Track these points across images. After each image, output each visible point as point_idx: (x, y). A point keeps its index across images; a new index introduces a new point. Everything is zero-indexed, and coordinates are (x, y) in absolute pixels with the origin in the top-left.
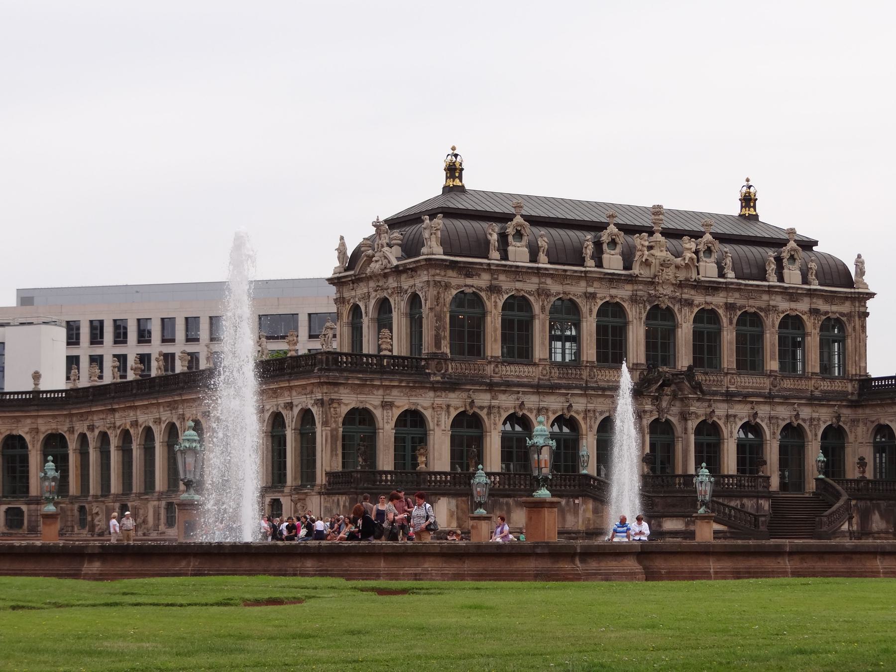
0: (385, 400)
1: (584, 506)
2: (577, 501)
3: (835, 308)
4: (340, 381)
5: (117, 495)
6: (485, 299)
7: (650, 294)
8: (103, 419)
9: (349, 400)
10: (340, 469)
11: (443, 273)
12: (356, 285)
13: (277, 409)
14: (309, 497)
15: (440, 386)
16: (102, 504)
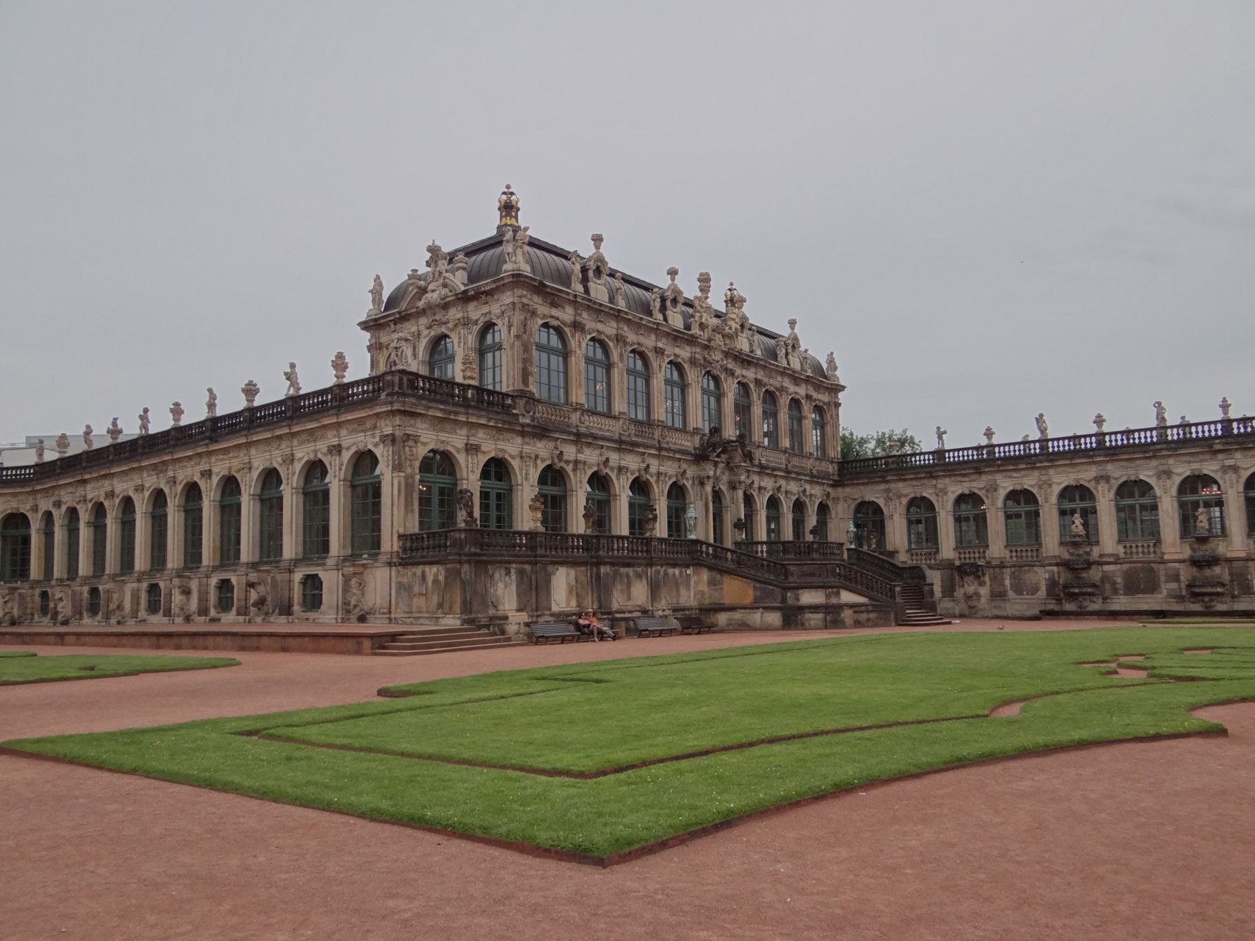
0: (471, 442)
1: (696, 577)
2: (688, 572)
3: (820, 397)
4: (418, 411)
5: (87, 578)
6: (569, 335)
7: (705, 359)
8: (71, 493)
9: (428, 438)
10: (416, 530)
11: (529, 296)
12: (399, 326)
13: (316, 455)
14: (368, 571)
15: (530, 430)
16: (67, 588)
